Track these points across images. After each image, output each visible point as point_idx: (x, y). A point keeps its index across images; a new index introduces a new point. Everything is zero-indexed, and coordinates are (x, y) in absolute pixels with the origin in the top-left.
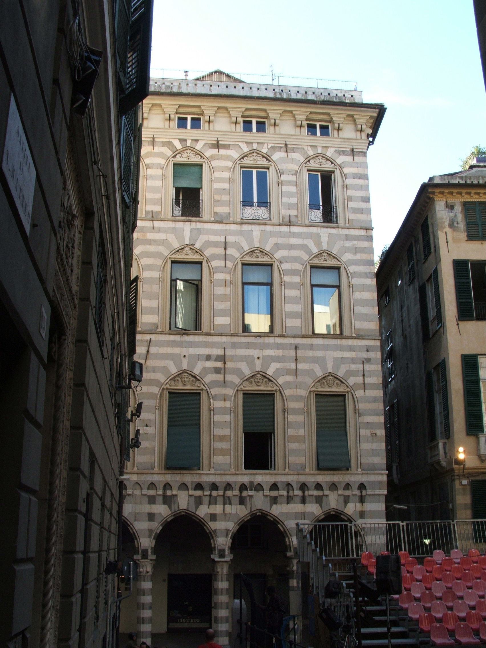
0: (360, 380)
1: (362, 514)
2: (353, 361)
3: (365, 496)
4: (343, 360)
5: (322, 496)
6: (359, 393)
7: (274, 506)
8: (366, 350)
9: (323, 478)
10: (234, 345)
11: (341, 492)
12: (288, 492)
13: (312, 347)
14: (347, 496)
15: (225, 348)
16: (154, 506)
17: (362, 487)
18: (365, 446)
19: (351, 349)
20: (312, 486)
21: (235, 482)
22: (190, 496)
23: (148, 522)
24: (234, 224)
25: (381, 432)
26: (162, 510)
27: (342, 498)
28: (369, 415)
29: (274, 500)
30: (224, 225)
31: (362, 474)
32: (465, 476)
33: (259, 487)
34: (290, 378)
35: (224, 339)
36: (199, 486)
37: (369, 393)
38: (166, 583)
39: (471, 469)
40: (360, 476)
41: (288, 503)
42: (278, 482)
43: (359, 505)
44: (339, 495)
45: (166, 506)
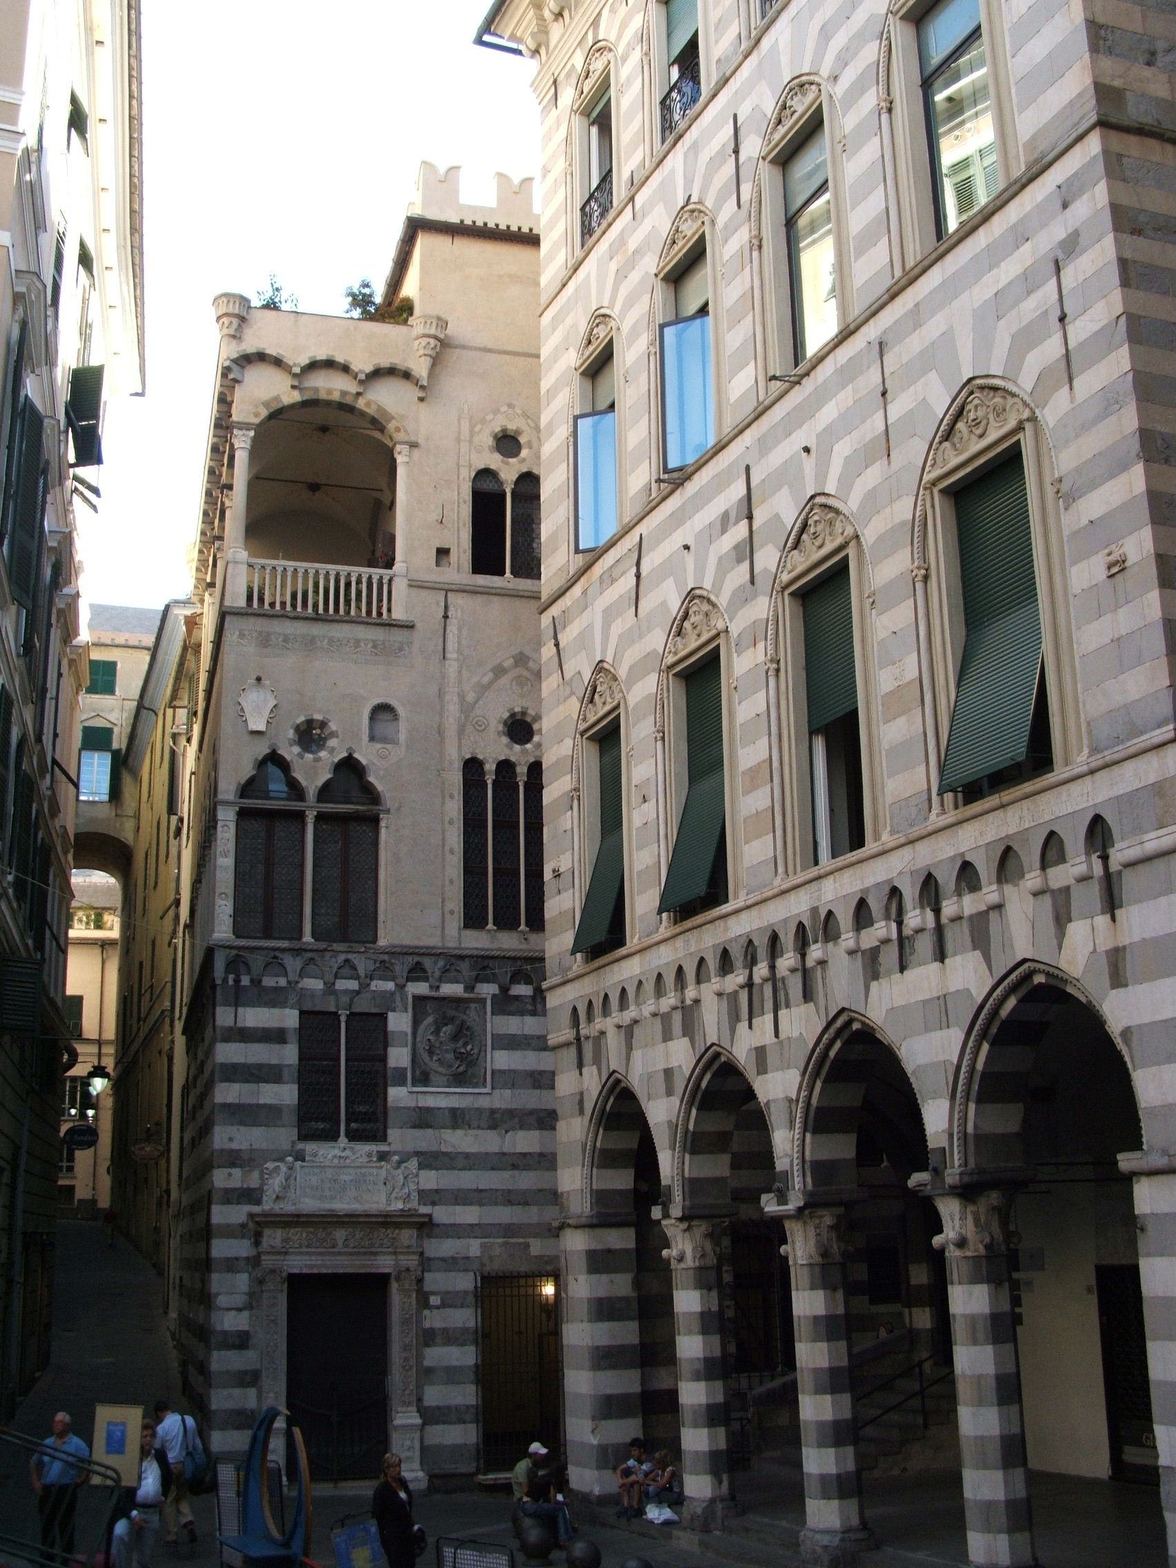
0: (1052, 349)
1: (1117, 967)
2: (1028, 283)
3: (1120, 873)
4: (1001, 302)
5: (987, 912)
7: (874, 984)
8: (1059, 205)
9: (978, 835)
10: (764, 446)
11: (1033, 880)
12: (900, 923)
13: (916, 318)
14: (1060, 890)
15: (748, 468)
16: (670, 1043)
17: (1098, 833)
18: (1091, 636)
19: (1020, 235)
20: (947, 878)
21: (785, 921)
22: (719, 994)
23: (665, 1100)
24: (746, 57)
25: (1139, 545)
26: (681, 1055)
27: (1047, 900)
28: (1093, 485)
29: (872, 964)
30: (732, 80)
31: (1092, 772)
33: (828, 927)
34: (873, 476)
36: (726, 963)
37: (1090, 382)
40: (1088, 779)
41: (902, 969)
42: (866, 891)
43: (1102, 921)
45: (686, 1039)
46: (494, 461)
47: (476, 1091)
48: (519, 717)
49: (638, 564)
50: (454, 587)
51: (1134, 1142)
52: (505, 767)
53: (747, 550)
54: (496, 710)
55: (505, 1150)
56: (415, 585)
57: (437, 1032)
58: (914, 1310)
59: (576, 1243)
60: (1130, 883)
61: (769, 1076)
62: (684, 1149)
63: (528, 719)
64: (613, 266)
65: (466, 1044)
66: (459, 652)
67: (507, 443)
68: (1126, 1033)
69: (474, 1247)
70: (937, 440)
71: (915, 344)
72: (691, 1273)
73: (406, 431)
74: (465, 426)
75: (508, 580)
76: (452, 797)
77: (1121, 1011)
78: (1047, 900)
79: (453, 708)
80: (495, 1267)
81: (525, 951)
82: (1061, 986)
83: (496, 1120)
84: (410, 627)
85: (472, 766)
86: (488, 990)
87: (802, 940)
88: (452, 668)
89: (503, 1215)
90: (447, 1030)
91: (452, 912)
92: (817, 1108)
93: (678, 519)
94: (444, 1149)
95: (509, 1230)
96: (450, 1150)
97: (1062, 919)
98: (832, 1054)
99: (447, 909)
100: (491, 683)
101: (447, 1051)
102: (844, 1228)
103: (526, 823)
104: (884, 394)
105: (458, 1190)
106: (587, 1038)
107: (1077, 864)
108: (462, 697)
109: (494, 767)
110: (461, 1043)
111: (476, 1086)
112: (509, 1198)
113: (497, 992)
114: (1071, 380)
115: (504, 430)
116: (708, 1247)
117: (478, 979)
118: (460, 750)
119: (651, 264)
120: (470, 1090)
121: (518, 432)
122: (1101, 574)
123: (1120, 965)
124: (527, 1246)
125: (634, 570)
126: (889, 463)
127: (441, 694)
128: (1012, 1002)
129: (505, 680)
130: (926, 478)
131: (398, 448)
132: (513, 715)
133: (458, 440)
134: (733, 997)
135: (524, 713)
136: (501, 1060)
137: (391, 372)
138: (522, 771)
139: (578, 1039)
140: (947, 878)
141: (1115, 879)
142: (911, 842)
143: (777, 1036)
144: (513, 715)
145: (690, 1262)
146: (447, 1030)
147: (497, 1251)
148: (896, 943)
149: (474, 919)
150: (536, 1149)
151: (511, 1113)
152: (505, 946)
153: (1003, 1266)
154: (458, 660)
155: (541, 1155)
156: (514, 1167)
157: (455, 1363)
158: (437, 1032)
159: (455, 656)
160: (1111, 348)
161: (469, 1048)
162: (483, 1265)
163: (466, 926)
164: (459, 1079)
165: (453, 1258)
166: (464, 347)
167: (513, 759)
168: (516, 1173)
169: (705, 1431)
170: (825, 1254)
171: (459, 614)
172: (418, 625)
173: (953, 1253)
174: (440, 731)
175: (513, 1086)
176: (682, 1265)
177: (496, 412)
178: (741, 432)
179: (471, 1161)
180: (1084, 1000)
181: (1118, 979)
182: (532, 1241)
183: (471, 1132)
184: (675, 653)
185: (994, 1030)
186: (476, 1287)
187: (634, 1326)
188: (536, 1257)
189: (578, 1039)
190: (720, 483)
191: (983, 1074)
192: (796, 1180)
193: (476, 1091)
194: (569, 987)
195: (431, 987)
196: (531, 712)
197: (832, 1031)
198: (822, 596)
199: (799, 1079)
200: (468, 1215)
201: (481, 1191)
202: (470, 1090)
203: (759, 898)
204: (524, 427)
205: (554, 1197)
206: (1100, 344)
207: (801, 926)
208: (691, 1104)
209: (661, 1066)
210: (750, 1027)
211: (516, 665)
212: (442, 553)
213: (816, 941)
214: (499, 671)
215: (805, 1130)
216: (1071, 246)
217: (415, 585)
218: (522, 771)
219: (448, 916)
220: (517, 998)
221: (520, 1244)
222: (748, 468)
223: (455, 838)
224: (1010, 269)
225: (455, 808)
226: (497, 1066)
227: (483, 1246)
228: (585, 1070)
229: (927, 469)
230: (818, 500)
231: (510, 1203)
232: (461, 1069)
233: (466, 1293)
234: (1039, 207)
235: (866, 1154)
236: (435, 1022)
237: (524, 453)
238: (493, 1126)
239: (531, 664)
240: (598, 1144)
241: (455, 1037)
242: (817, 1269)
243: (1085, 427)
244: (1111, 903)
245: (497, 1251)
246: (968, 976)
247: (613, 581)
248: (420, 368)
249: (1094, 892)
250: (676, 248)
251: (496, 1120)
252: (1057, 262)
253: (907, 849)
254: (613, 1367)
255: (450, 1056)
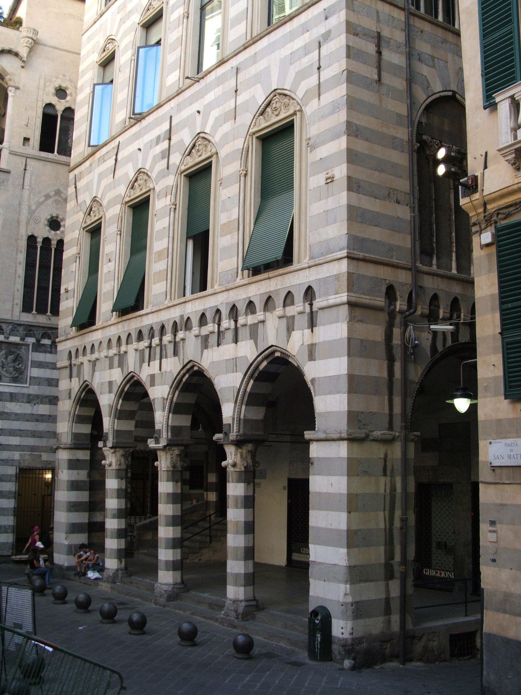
0: (313, 81)
1: (312, 352)
2: (306, 50)
3: (317, 312)
4: (293, 57)
5: (258, 323)
6: (311, 108)
7: (205, 351)
8: (324, 18)
10: (180, 108)
11: (279, 311)
12: (219, 325)
13: (254, 59)
14: (290, 317)
15: (171, 117)
16: (112, 370)
17: (309, 293)
19: (305, 29)
20: (242, 308)
21: (169, 320)
22: (136, 350)
23: (108, 395)
25: (341, 171)
26: (117, 376)
27: (284, 320)
28: (324, 143)
29: (205, 342)
31: (309, 267)
32: (488, 220)
33: (187, 324)
34: (227, 127)
35: (173, 103)
36: (140, 336)
38: (286, 492)
39: (503, 196)
41: (218, 345)
42: (206, 309)
43: (307, 331)
44: (280, 318)
45: (120, 369)
46: (54, 100)
47: (22, 385)
48: (55, 219)
49: (117, 155)
50: (30, 156)
51: (312, 427)
52: (47, 241)
53: (167, 154)
54: (45, 215)
55: (33, 413)
56: (12, 153)
57: (6, 358)
58: (209, 493)
59: (63, 456)
60: (321, 317)
61: (155, 387)
62: (115, 417)
63: (59, 220)
64: (119, 16)
65: (19, 364)
66: (30, 186)
67: (61, 93)
68: (313, 380)
69: (16, 455)
70: (257, 114)
71: (253, 70)
72: (114, 471)
73: (14, 81)
74: (42, 81)
75: (55, 156)
76: (21, 252)
77: (311, 371)
78: (284, 320)
79: (25, 211)
80: (25, 465)
81: (49, 324)
82: (287, 358)
83: (30, 399)
84: (8, 172)
85: (32, 239)
86: (31, 340)
87: (175, 328)
88: (26, 193)
89: (30, 441)
90: (11, 357)
91: (17, 304)
92: (176, 403)
93: (137, 136)
94: (6, 411)
95: (33, 449)
96: (8, 411)
97: (290, 329)
98: (184, 380)
99: (15, 303)
100: (43, 202)
101: (10, 367)
102: (183, 456)
103: (54, 267)
104: (236, 91)
105: (11, 430)
106: (75, 365)
107: (299, 306)
108: (29, 207)
109: (41, 240)
110: (17, 363)
111: (22, 383)
112: (34, 434)
113: (35, 341)
114: (319, 95)
115: (60, 87)
116: (123, 460)
117: (27, 335)
118: (26, 231)
119: (137, 18)
120: (20, 385)
121: (66, 88)
122: (323, 182)
123: (313, 352)
124: (41, 456)
125: (114, 157)
126: (235, 122)
127: (20, 204)
128: (265, 363)
129: (50, 201)
130: (251, 131)
131: (10, 88)
132: (52, 217)
133: (38, 88)
134: (142, 352)
135: (57, 217)
136: (35, 372)
137: (9, 52)
138: (54, 243)
139: (71, 365)
140: (242, 308)
141: (314, 314)
142: (228, 290)
143: (160, 370)
144: (52, 217)
145: (114, 466)
146: (11, 357)
147: (27, 457)
148: (217, 334)
149: (27, 308)
150: (47, 413)
151: (37, 396)
152: (40, 321)
153: (250, 476)
154: (29, 190)
155: (50, 416)
156: (37, 420)
157: (5, 506)
158: (6, 358)
159: (28, 188)
160: (338, 84)
161: (20, 366)
162: (20, 463)
163: (23, 311)
164: (15, 380)
165: (7, 460)
166: (45, 45)
167: (50, 237)
168: (38, 423)
169: (116, 540)
170: (174, 467)
171: (32, 169)
172: (12, 172)
173: (230, 469)
174: (18, 222)
175: (39, 384)
176: (110, 468)
177: (57, 77)
178: (170, 100)
179: (18, 417)
180: (296, 365)
181: (311, 357)
182: (43, 454)
183: (19, 404)
184: (130, 197)
185: (256, 375)
186: (16, 473)
187: (87, 493)
188: (44, 461)
189: (71, 365)
190: (158, 122)
191: (250, 393)
192: (164, 434)
193: (22, 385)
194: (68, 342)
195: (5, 337)
196: (61, 217)
197: (185, 370)
198: (199, 177)
199: (168, 390)
200: (15, 441)
201: (22, 430)
202: (20, 385)
203: (157, 309)
204: (69, 86)
205: (54, 435)
206: (334, 82)
207: (175, 323)
208: (119, 397)
209: (107, 380)
210: (149, 365)
211: (56, 195)
212: (26, 140)
213: (181, 330)
214: (48, 197)
215: (170, 412)
216: (327, 36)
217: (12, 153)
218: (54, 243)
219: (15, 306)
220: (44, 345)
221: (37, 455)
222: (171, 117)
223: (21, 271)
224: (299, 43)
225: (22, 257)
226: (32, 375)
227: (20, 455)
228: (73, 379)
229: (251, 127)
230: (201, 135)
231: (34, 436)
232: (16, 375)
233: (11, 475)
234: (315, 18)
235: (194, 425)
236: (6, 353)
237: (68, 98)
238: (29, 402)
239: (62, 195)
240: (76, 413)
241: (14, 361)
242: (170, 473)
243: (323, 117)
244: (312, 324)
245: (27, 457)
246: (247, 351)
247: (104, 161)
248: (23, 52)
249: (305, 319)
250: (149, 12)
251: (30, 399)
252: (320, 43)
253: (226, 293)
254: (77, 511)
255: (12, 369)
